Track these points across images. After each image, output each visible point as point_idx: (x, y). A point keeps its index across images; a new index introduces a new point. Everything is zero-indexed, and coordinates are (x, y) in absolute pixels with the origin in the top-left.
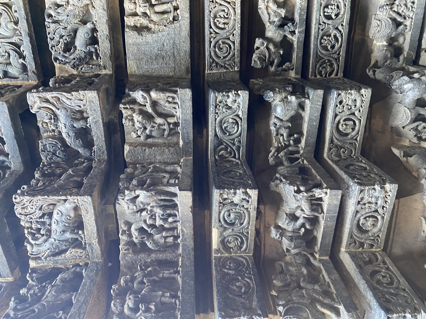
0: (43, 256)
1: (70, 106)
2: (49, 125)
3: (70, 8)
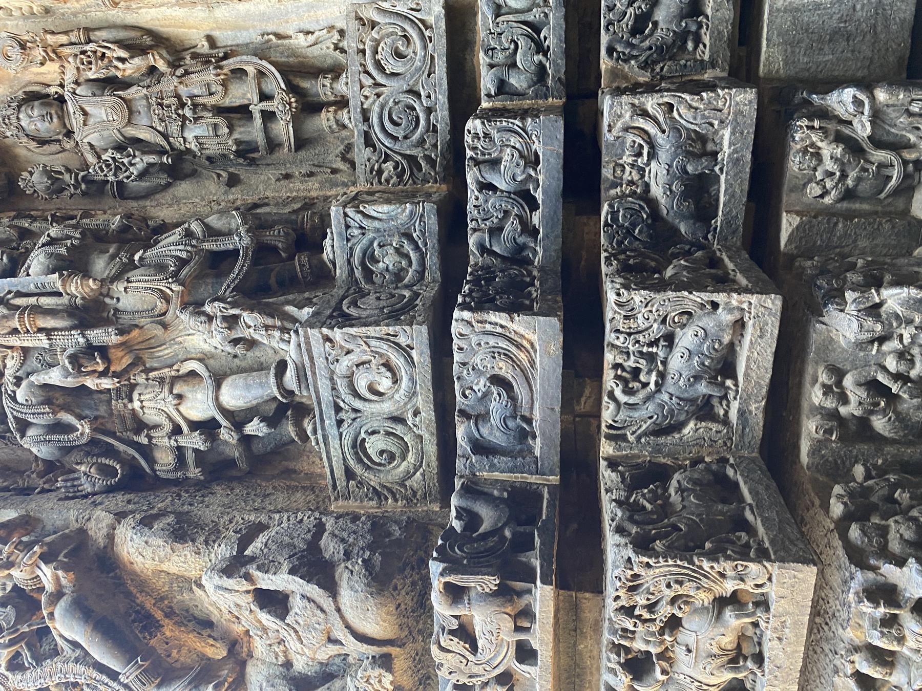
0: (634, 433)
1: (692, 123)
2: (628, 168)
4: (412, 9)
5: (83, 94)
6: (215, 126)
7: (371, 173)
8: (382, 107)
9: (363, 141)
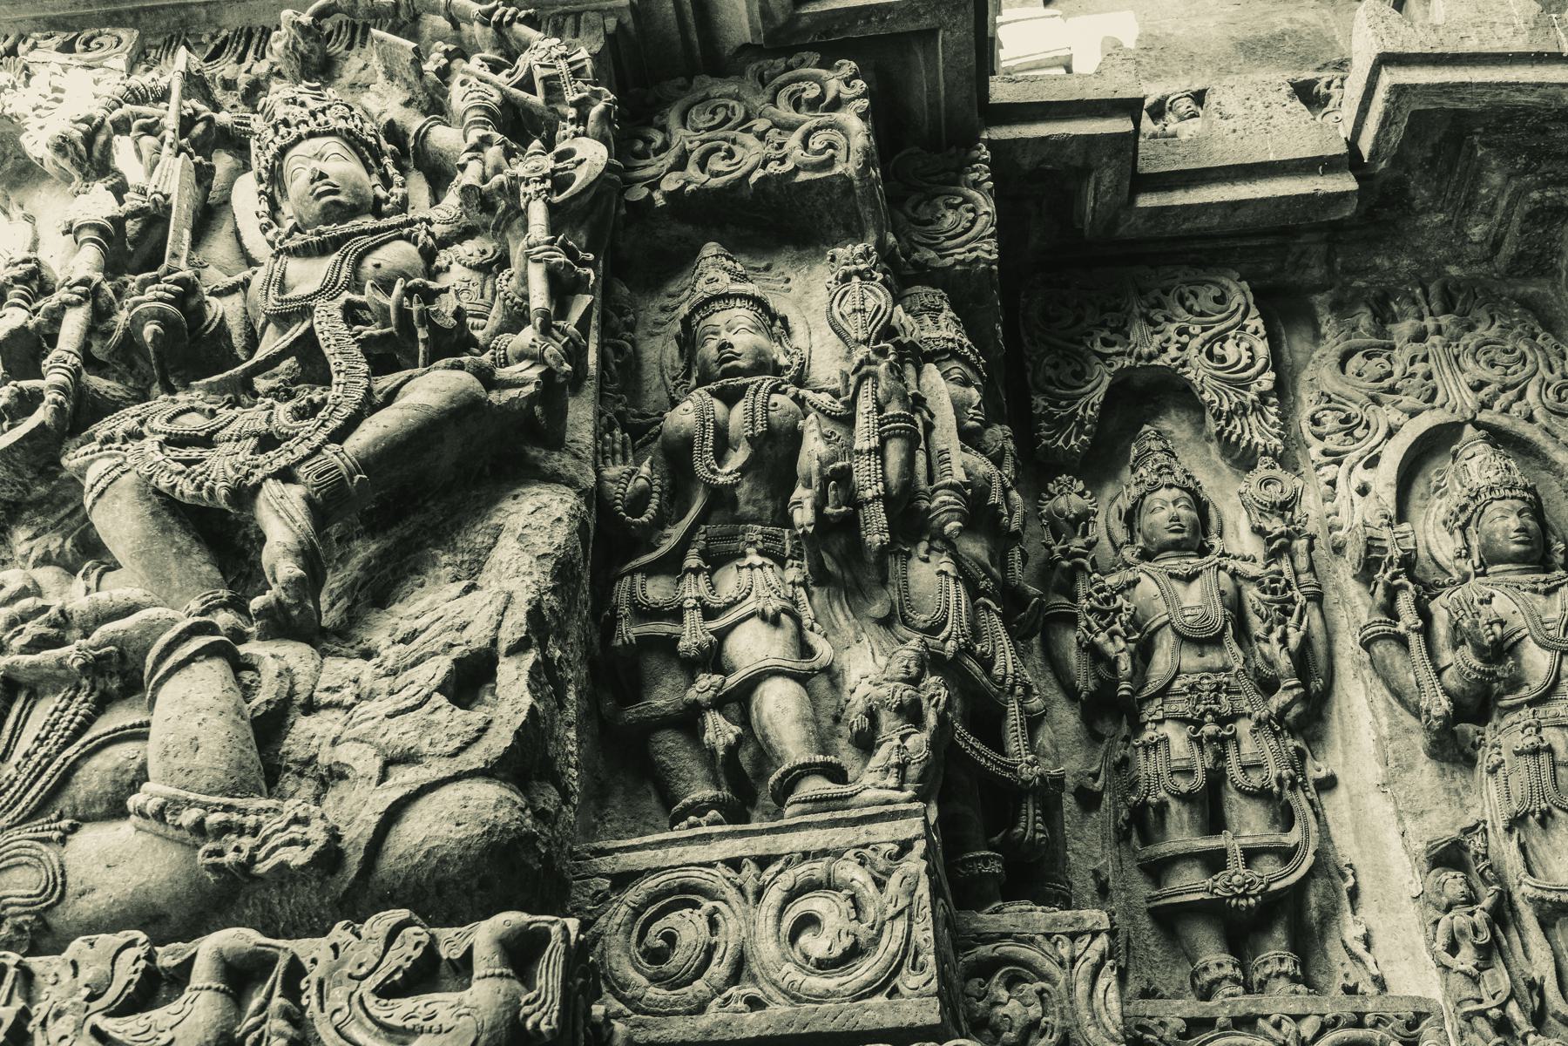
6: (1188, 772)
7: (1140, 1027)
9: (1197, 1014)
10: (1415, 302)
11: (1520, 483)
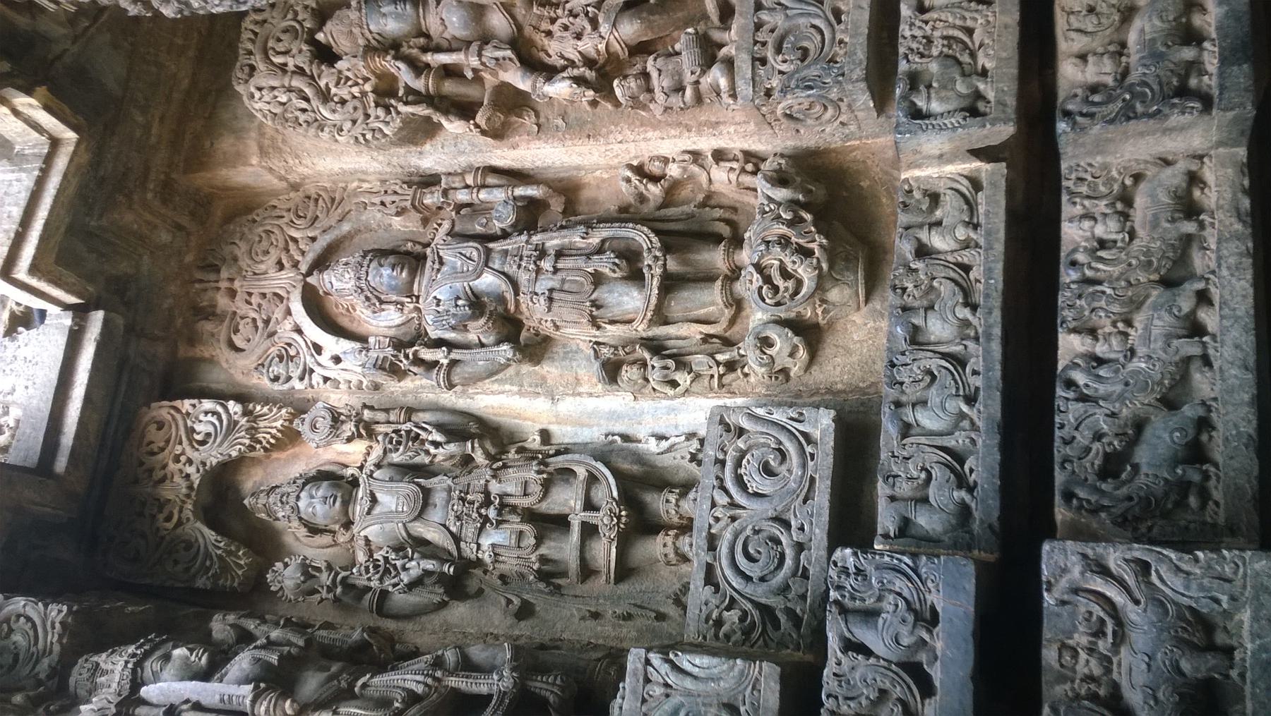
1: (1183, 595)
2: (1083, 656)
3: (1139, 364)
4: (792, 419)
5: (380, 478)
6: (521, 534)
7: (707, 621)
8: (736, 536)
9: (702, 575)
10: (205, 290)
11: (359, 259)
